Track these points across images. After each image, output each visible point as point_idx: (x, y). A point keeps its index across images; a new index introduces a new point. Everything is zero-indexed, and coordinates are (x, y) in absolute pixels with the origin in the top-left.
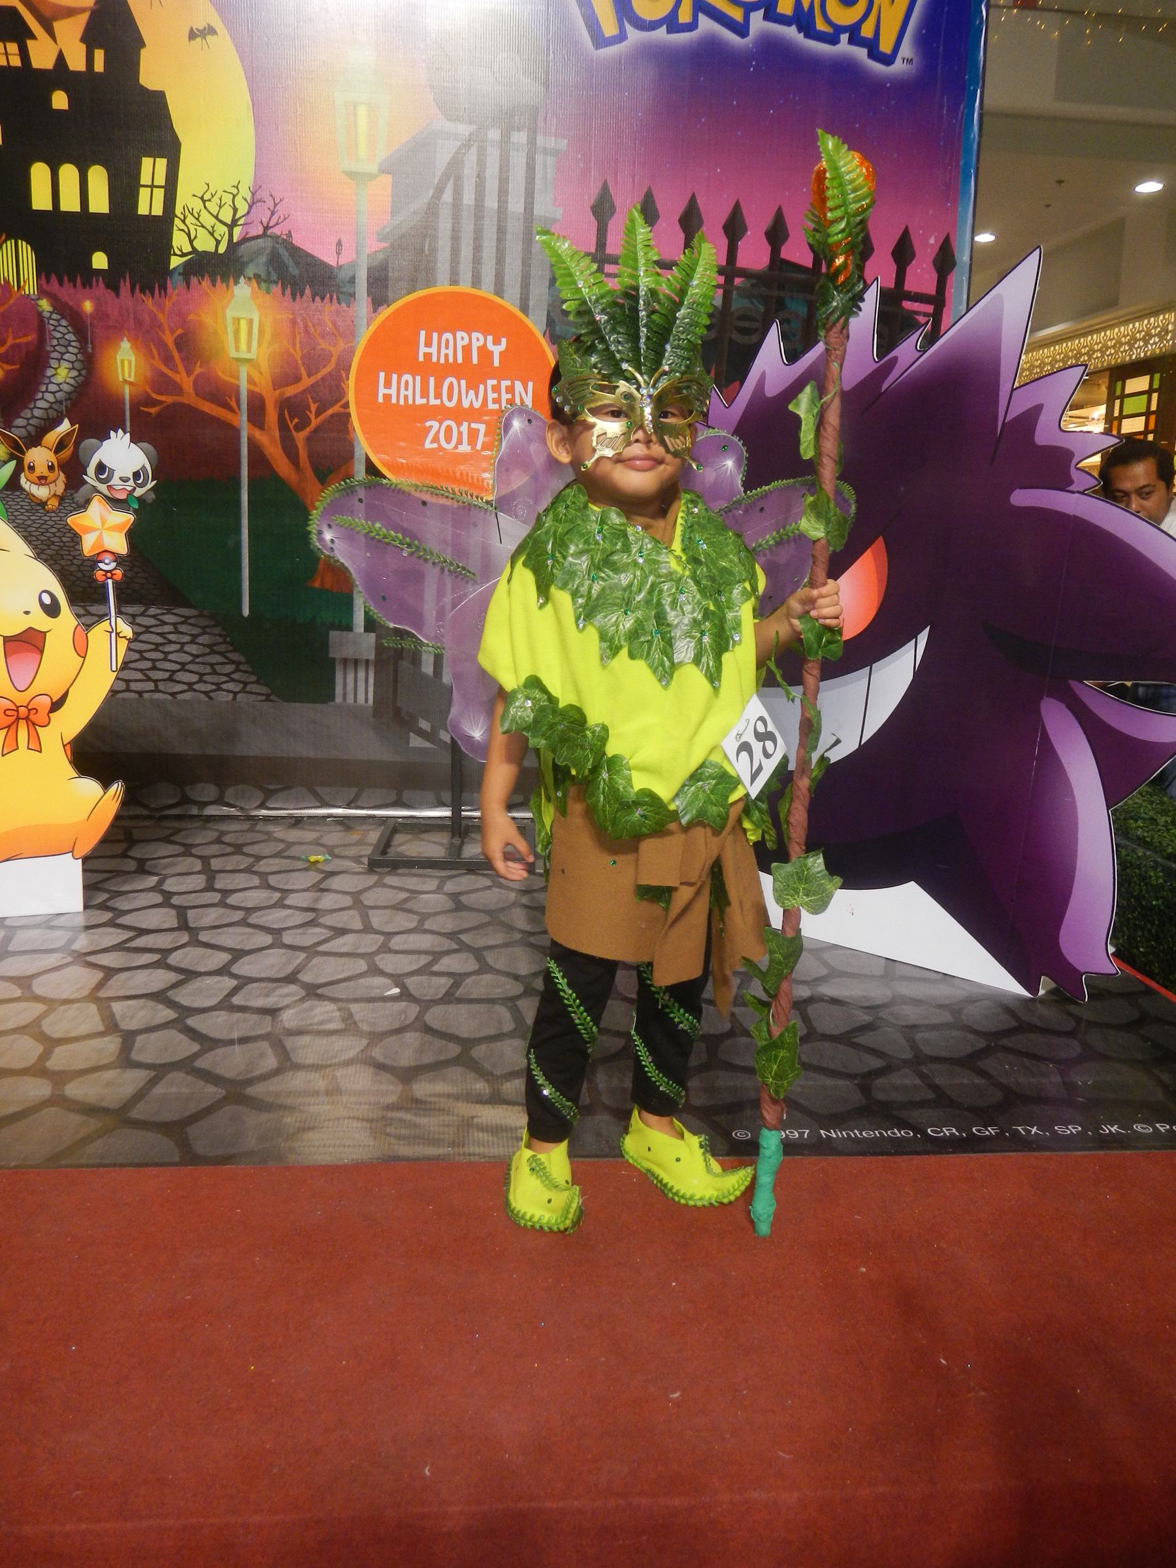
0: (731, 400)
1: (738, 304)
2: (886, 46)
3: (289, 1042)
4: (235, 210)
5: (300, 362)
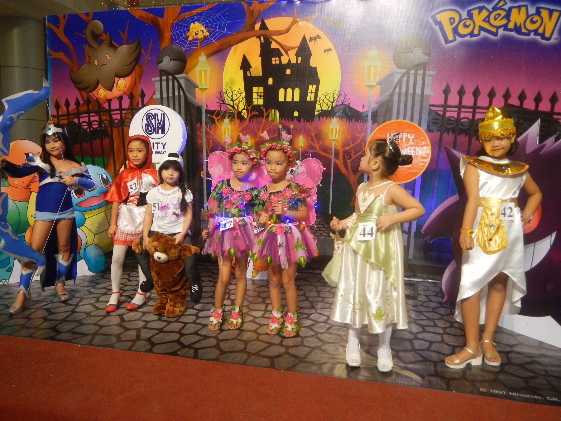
2: (547, 35)
4: (334, 98)
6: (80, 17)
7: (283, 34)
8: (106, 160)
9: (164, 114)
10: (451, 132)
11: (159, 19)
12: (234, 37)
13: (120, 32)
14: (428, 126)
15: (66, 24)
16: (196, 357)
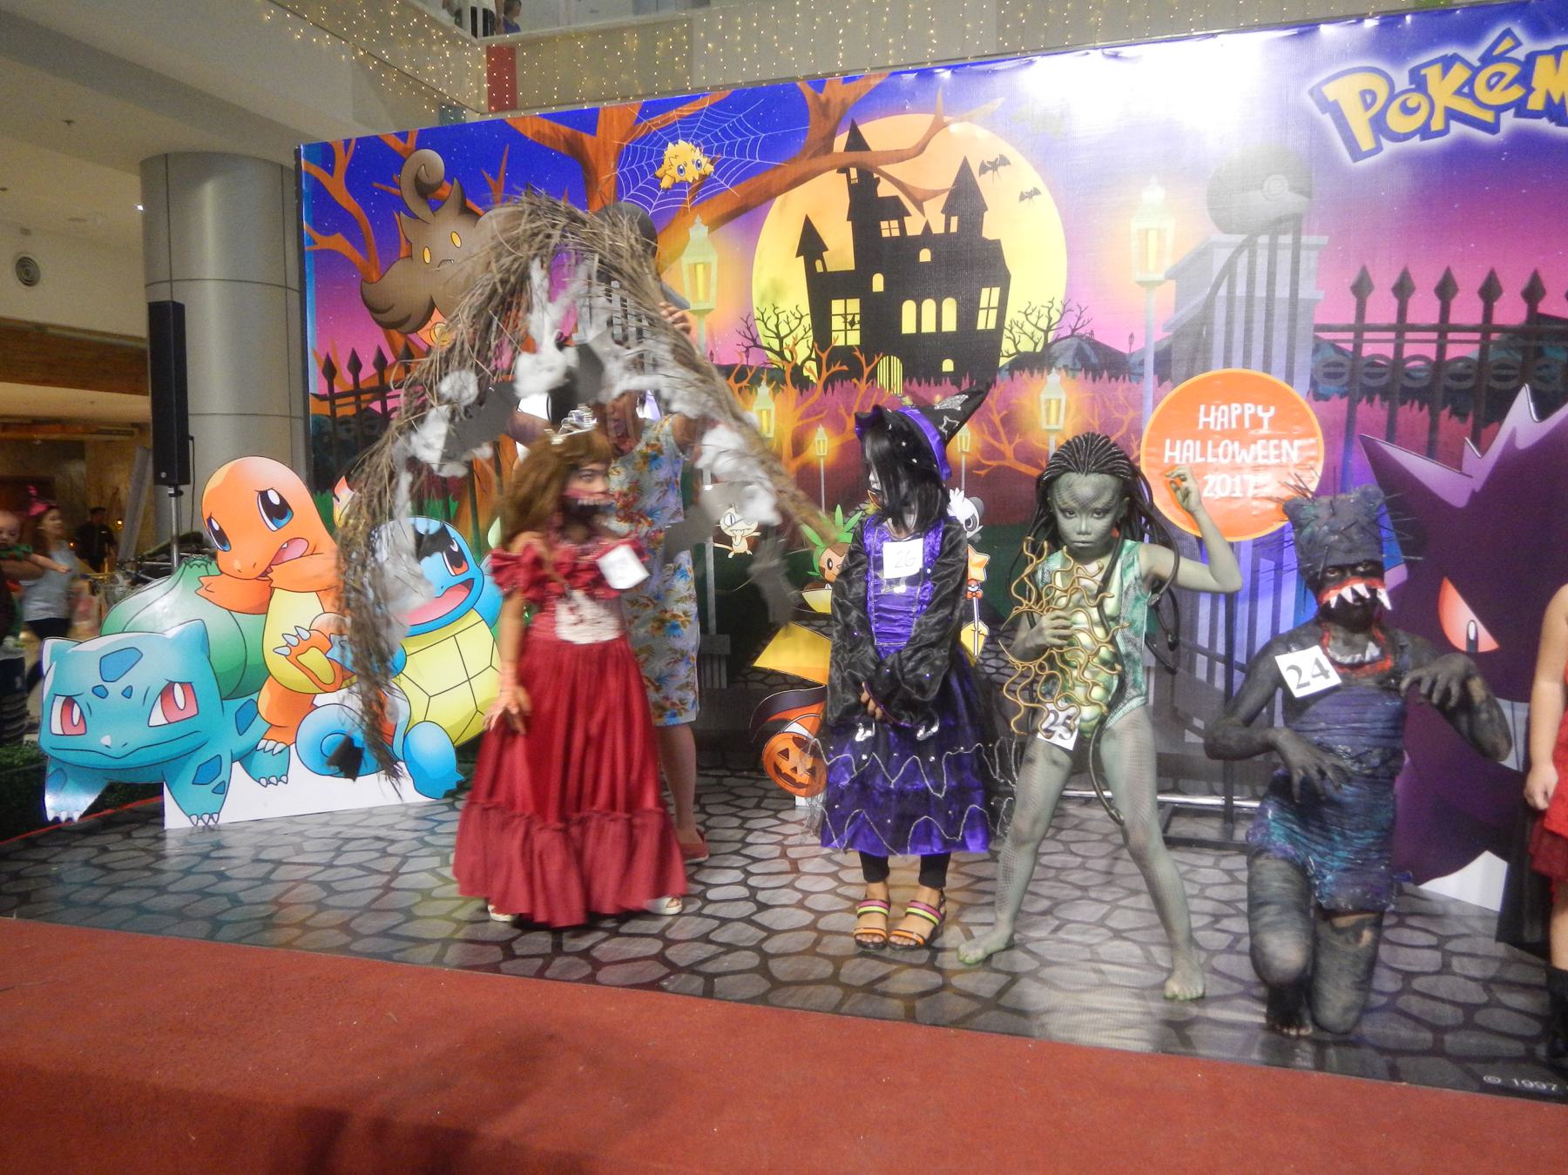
0: (1483, 451)
1: (1494, 356)
4: (1050, 319)
6: (385, 145)
8: (453, 506)
10: (1377, 397)
11: (586, 137)
12: (779, 172)
13: (488, 176)
14: (1314, 384)
15: (351, 162)
16: (708, 993)
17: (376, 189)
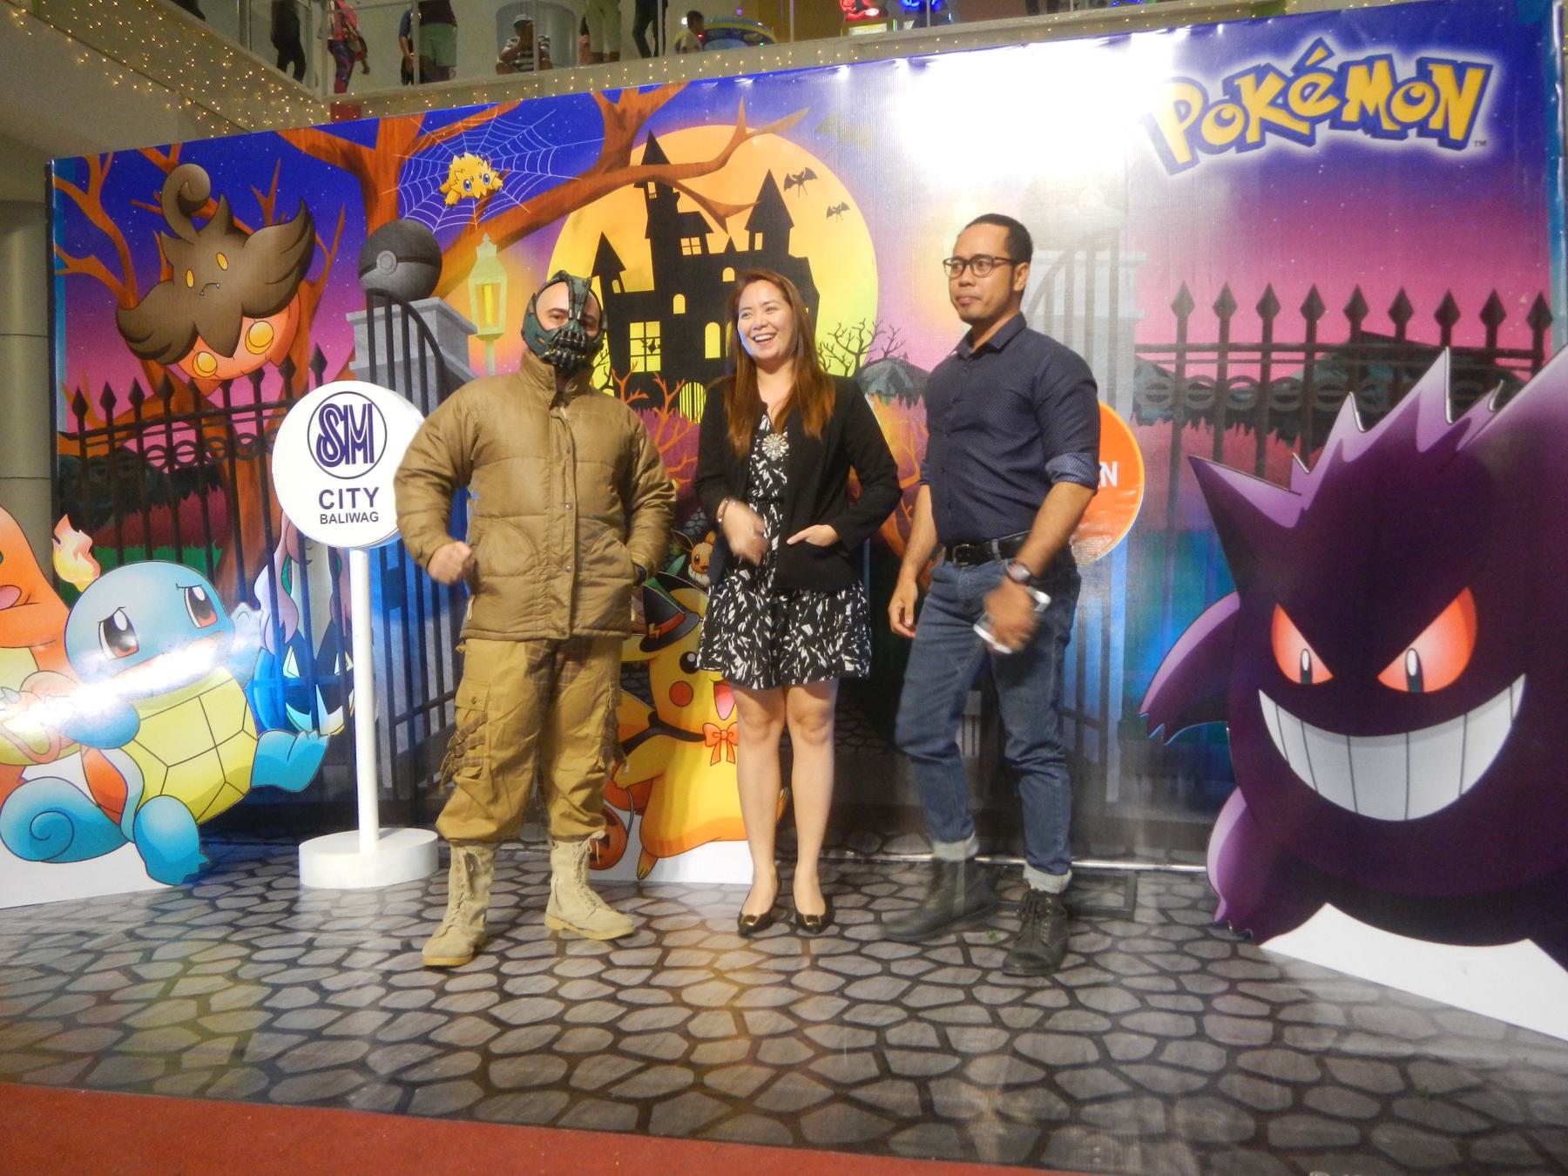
1: (1320, 376)
2: (1456, 133)
3: (891, 1056)
4: (862, 342)
5: (913, 457)
7: (709, 172)
8: (217, 554)
9: (370, 407)
11: (365, 151)
12: (572, 186)
14: (1137, 408)
17: (137, 208)
